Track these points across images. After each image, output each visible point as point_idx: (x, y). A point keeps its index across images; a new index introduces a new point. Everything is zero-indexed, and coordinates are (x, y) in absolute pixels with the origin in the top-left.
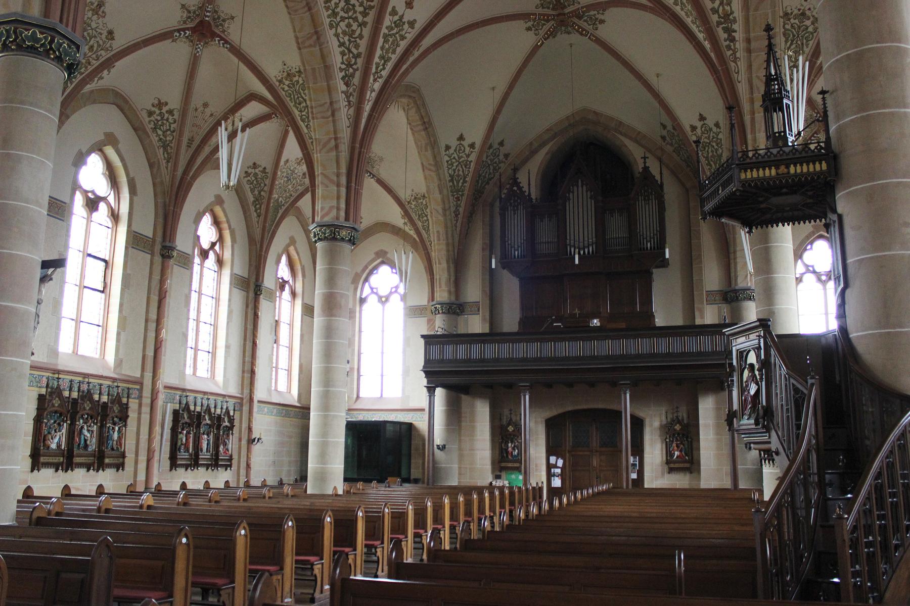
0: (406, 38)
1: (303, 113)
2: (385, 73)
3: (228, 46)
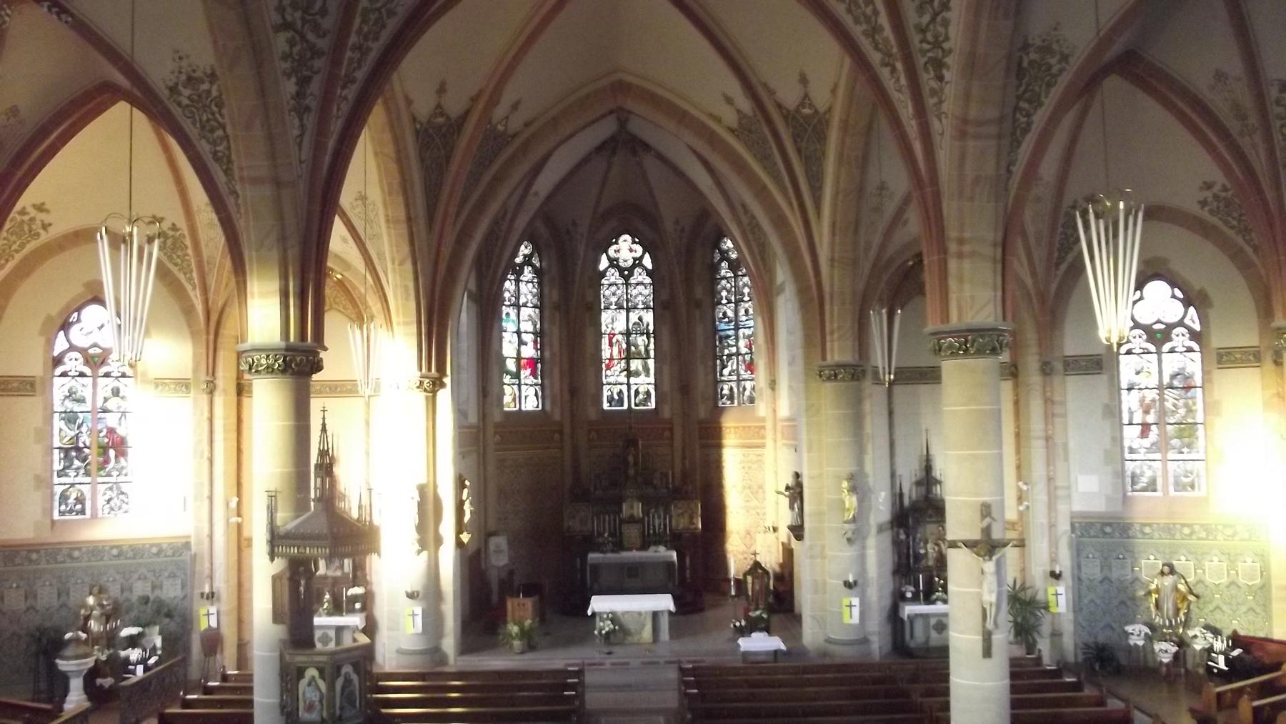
1: (218, 148)
2: (360, 75)
3: (70, 19)
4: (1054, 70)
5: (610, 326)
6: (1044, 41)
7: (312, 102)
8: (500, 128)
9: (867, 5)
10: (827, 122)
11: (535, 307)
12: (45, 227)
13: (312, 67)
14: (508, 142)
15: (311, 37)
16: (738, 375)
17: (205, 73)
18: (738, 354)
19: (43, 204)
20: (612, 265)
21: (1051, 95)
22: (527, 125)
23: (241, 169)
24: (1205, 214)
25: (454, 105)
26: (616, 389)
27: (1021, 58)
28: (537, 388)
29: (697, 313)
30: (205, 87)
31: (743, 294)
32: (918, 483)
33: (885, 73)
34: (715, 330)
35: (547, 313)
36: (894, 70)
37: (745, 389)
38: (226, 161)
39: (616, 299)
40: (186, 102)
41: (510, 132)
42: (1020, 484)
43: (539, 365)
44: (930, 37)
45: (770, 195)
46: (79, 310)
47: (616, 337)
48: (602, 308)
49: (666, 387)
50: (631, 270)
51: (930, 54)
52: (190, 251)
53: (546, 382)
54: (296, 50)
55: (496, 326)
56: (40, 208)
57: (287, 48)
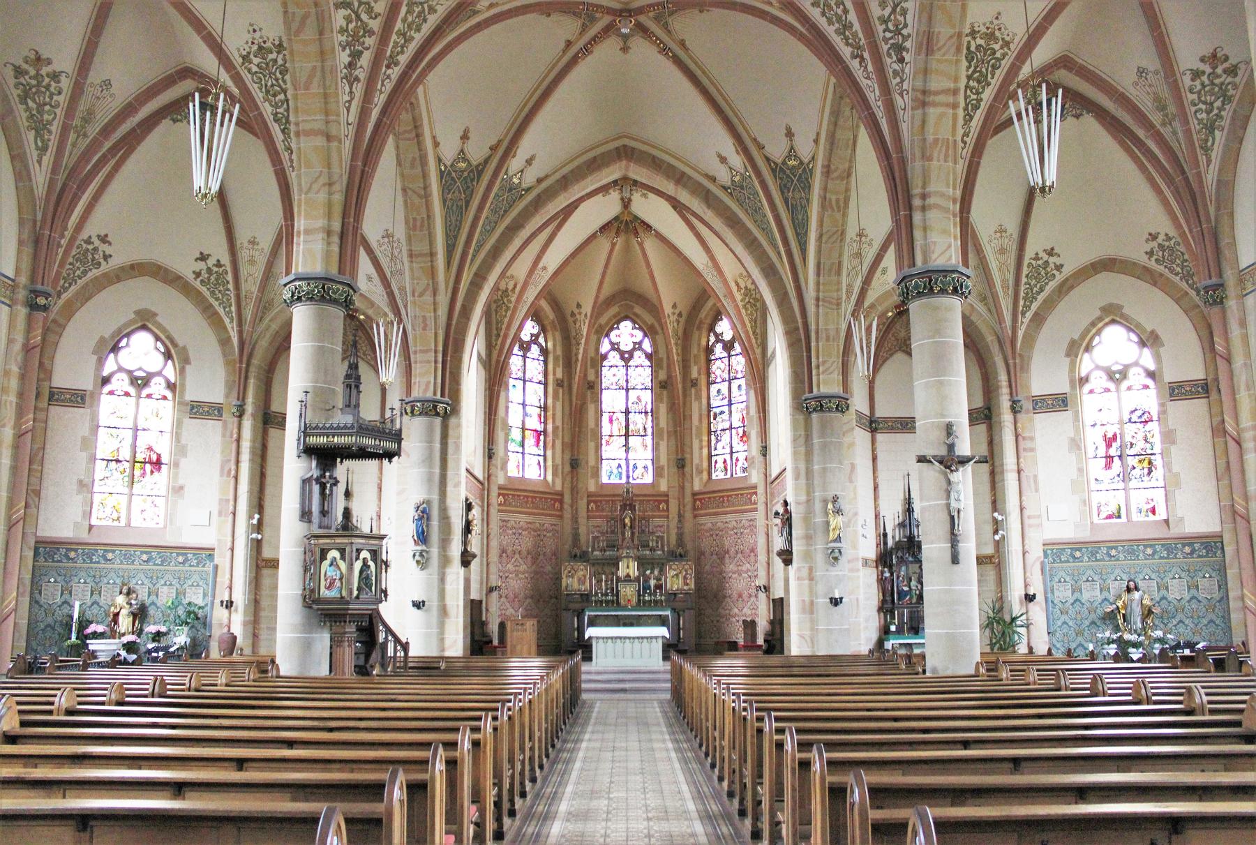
0: (435, 11)
2: (404, 59)
4: (998, 55)
6: (988, 28)
7: (362, 74)
8: (515, 180)
9: (838, 5)
10: (811, 171)
11: (540, 383)
12: (106, 257)
13: (364, 43)
14: (522, 195)
15: (364, 17)
16: (731, 448)
17: (274, 45)
18: (731, 428)
19: (106, 236)
20: (613, 349)
21: (996, 77)
22: (539, 181)
23: (297, 124)
24: (1152, 264)
25: (477, 151)
26: (615, 464)
27: (969, 42)
29: (693, 391)
30: (271, 56)
31: (737, 372)
32: (902, 525)
33: (854, 64)
34: (709, 407)
35: (550, 389)
36: (862, 59)
37: (737, 460)
38: (284, 121)
40: (255, 69)
41: (524, 186)
42: (996, 515)
43: (542, 437)
44: (891, 27)
45: (760, 245)
46: (128, 335)
49: (663, 461)
50: (631, 353)
51: (892, 41)
52: (231, 286)
53: (549, 453)
54: (351, 26)
55: (503, 394)
56: (104, 239)
57: (344, 25)
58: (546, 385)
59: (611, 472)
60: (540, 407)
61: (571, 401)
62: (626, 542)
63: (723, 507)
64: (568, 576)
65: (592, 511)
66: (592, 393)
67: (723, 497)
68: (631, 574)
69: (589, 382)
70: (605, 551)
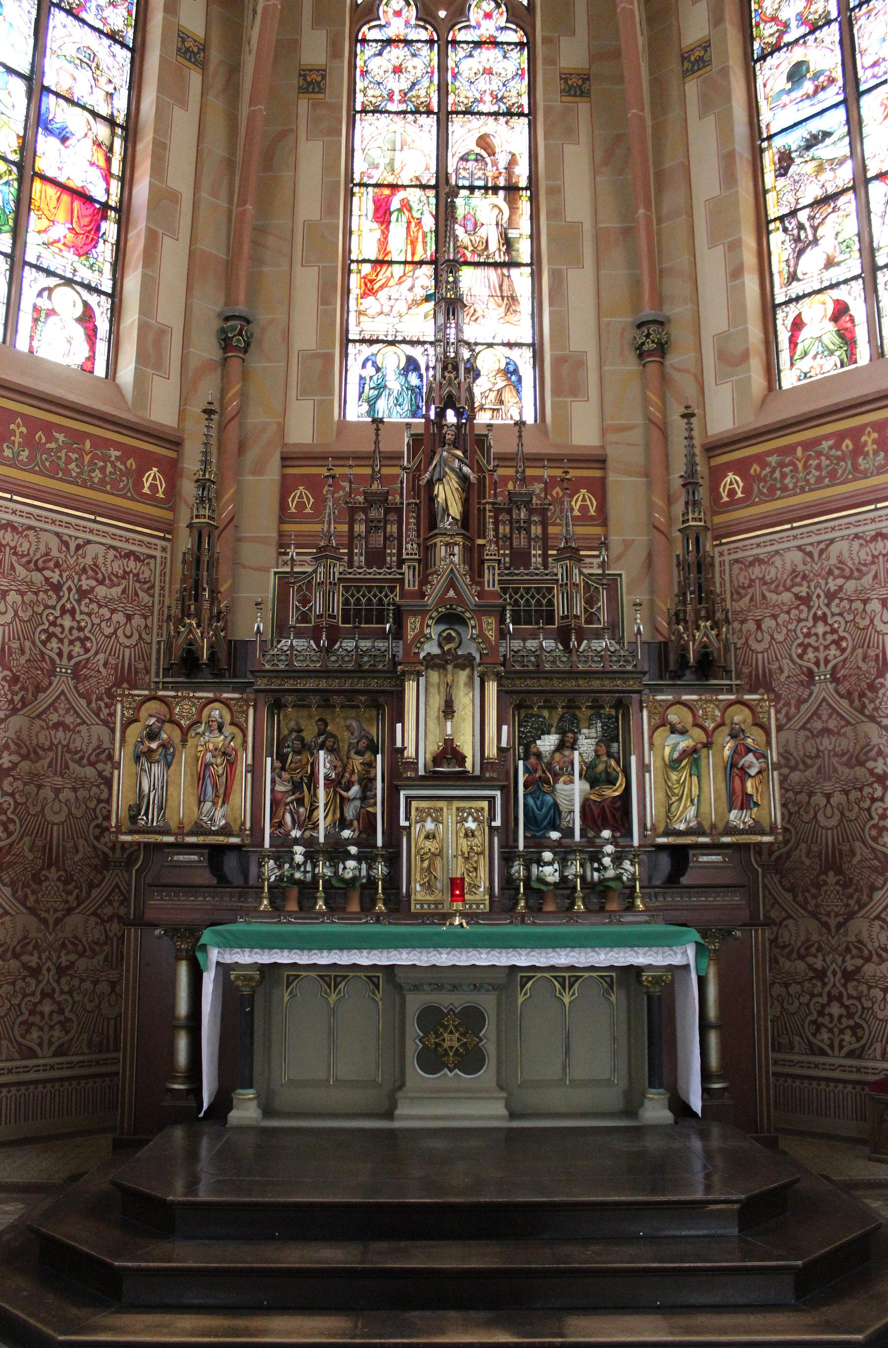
5: (383, 162)
11: (113, 37)
28: (93, 299)
39: (405, 85)
43: (109, 228)
47: (401, 195)
48: (358, 107)
53: (132, 283)
58: (137, 53)
59: (381, 388)
60: (111, 121)
61: (232, 119)
62: (438, 583)
63: (859, 474)
64: (142, 756)
65: (300, 517)
66: (315, 106)
67: (856, 433)
68: (467, 745)
69: (303, 73)
70: (334, 635)
